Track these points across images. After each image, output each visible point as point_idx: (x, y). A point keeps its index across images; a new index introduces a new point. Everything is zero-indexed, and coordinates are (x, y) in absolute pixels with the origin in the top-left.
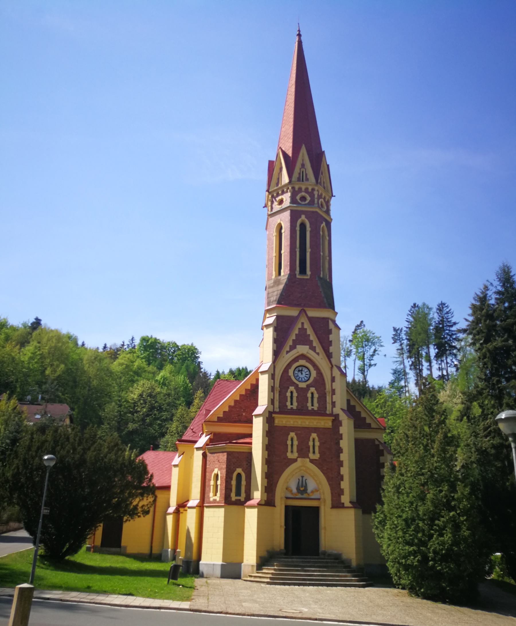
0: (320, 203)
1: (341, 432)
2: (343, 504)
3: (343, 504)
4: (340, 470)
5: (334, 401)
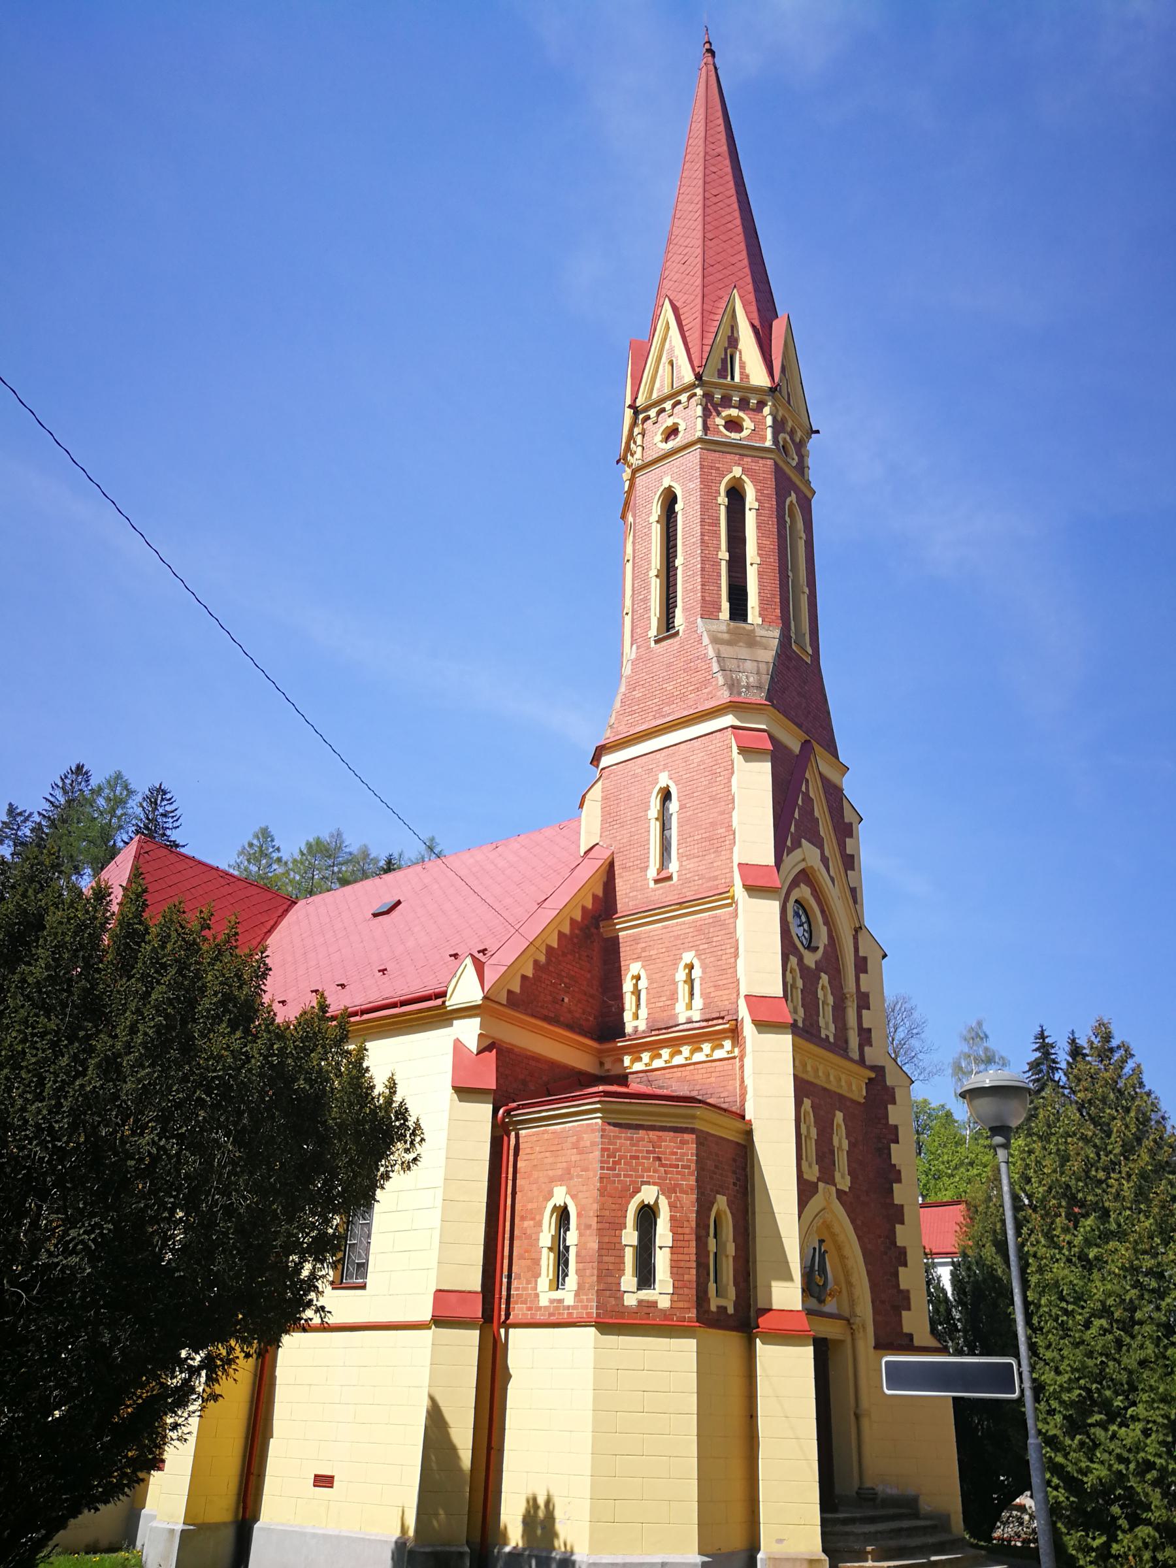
0: (781, 443)
1: (892, 1121)
2: (910, 1336)
3: (910, 1336)
4: (893, 1231)
5: (865, 1025)
